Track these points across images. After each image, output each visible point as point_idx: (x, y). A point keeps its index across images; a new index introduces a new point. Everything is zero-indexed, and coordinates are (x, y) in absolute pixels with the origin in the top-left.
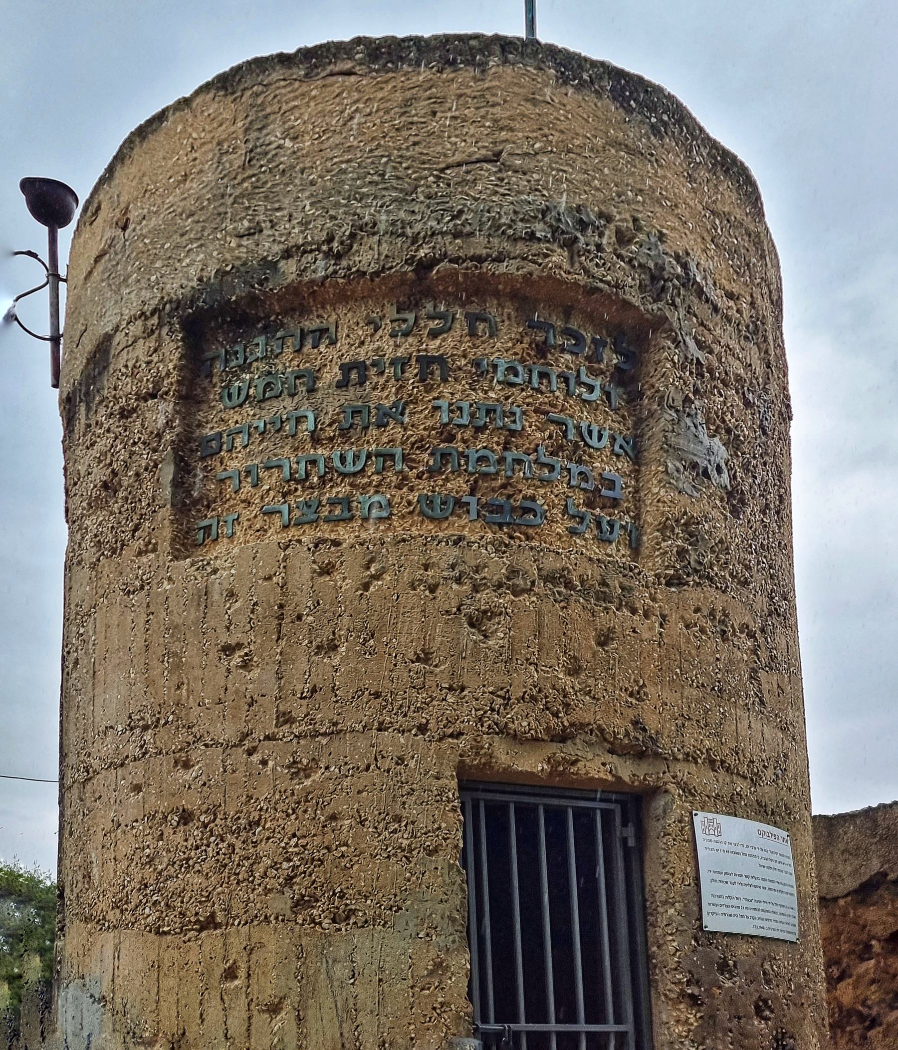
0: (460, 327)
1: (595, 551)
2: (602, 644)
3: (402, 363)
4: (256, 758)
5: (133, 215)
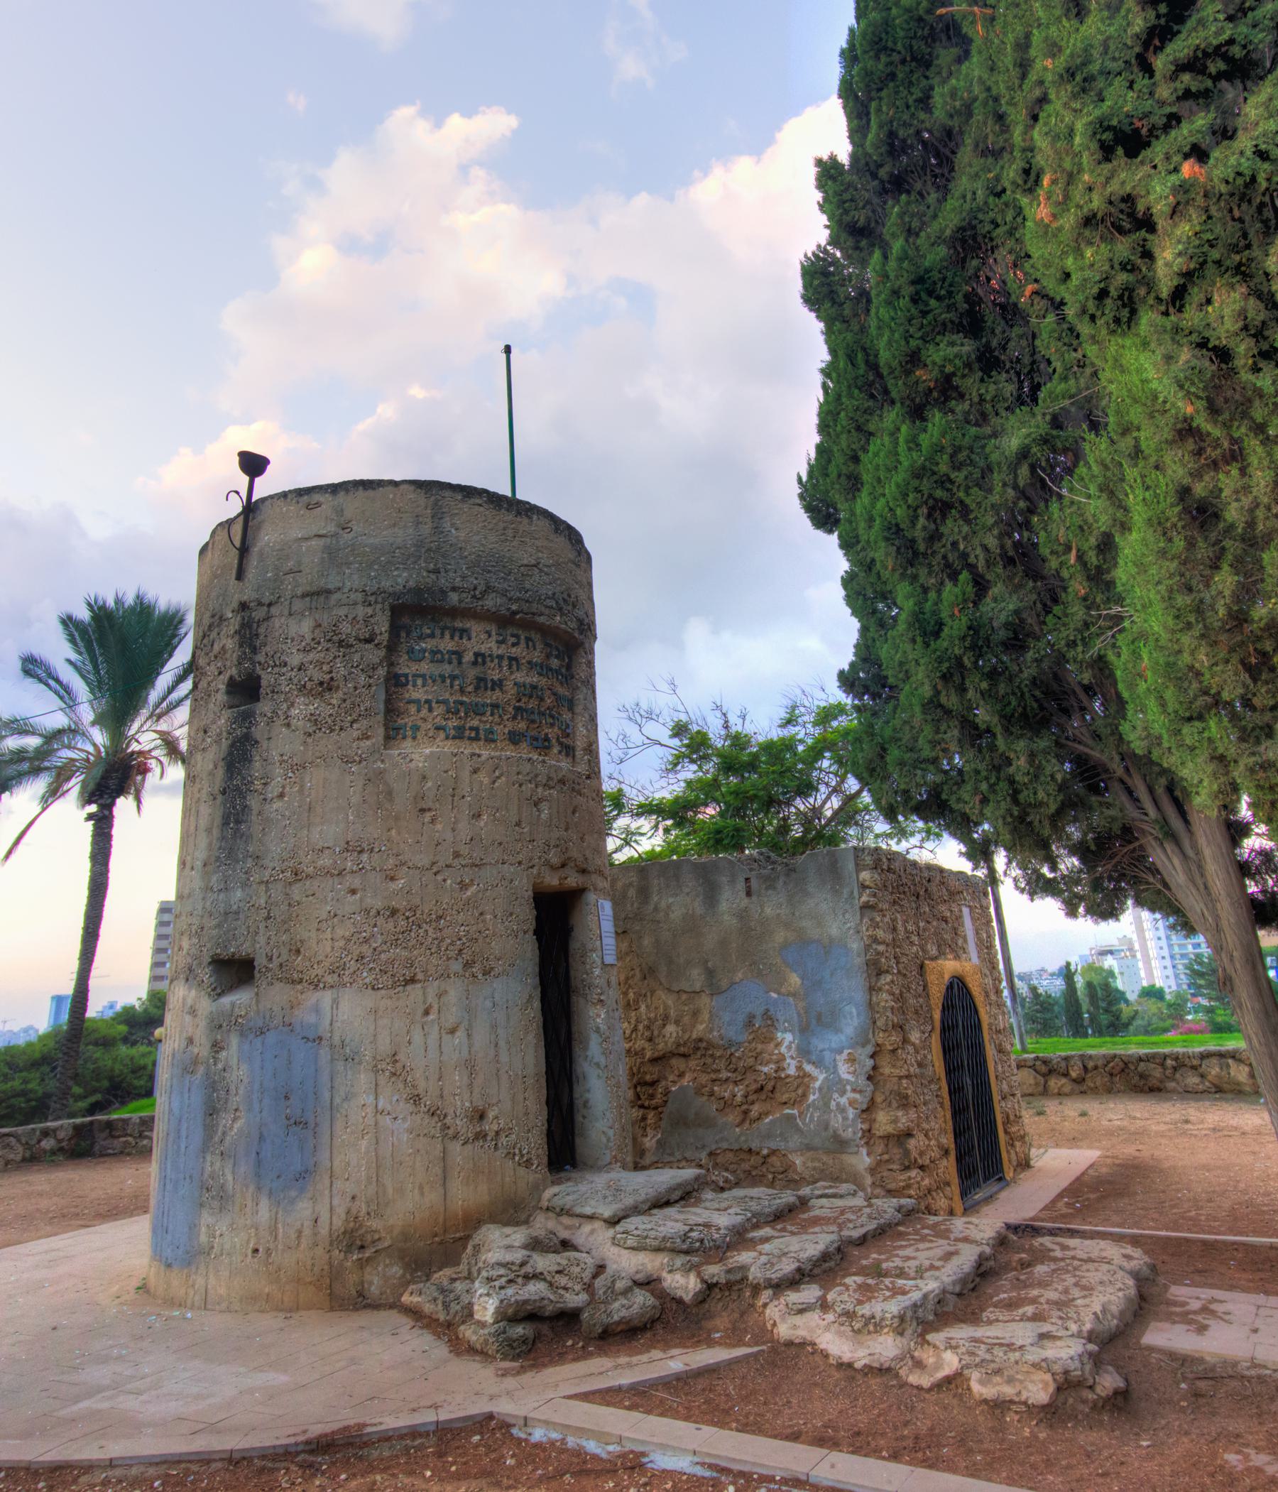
3: (500, 657)
4: (439, 878)
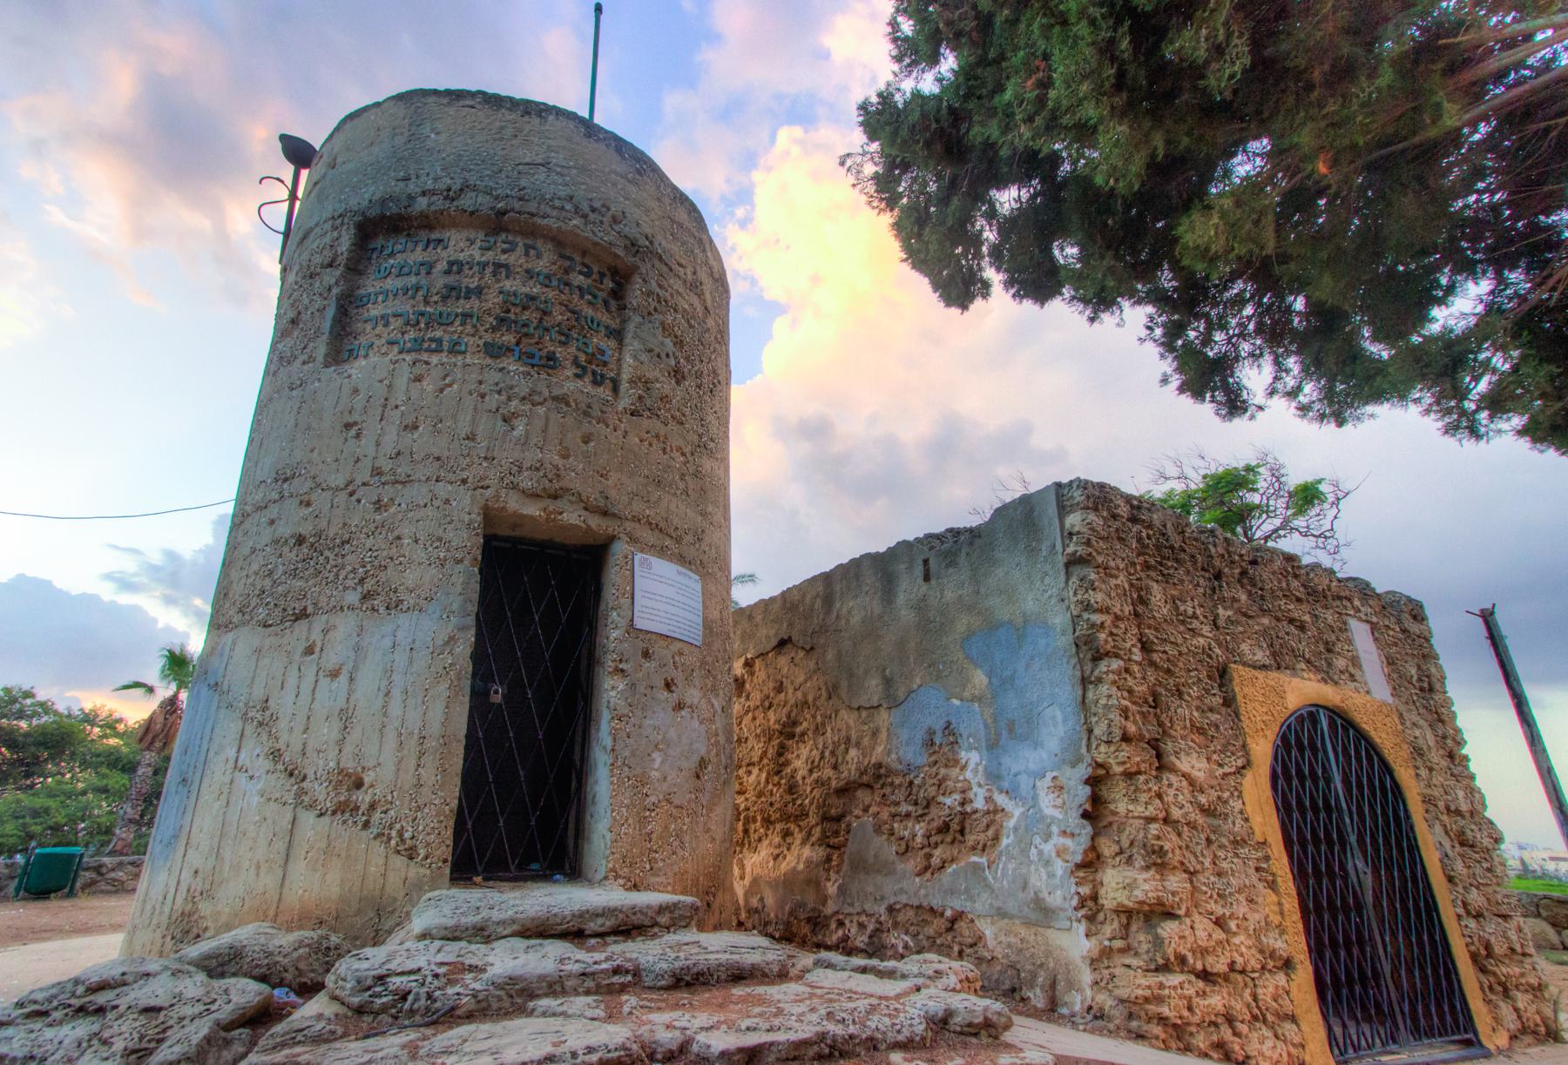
0: (520, 249)
1: (589, 389)
2: (586, 443)
3: (484, 265)
5: (339, 160)
